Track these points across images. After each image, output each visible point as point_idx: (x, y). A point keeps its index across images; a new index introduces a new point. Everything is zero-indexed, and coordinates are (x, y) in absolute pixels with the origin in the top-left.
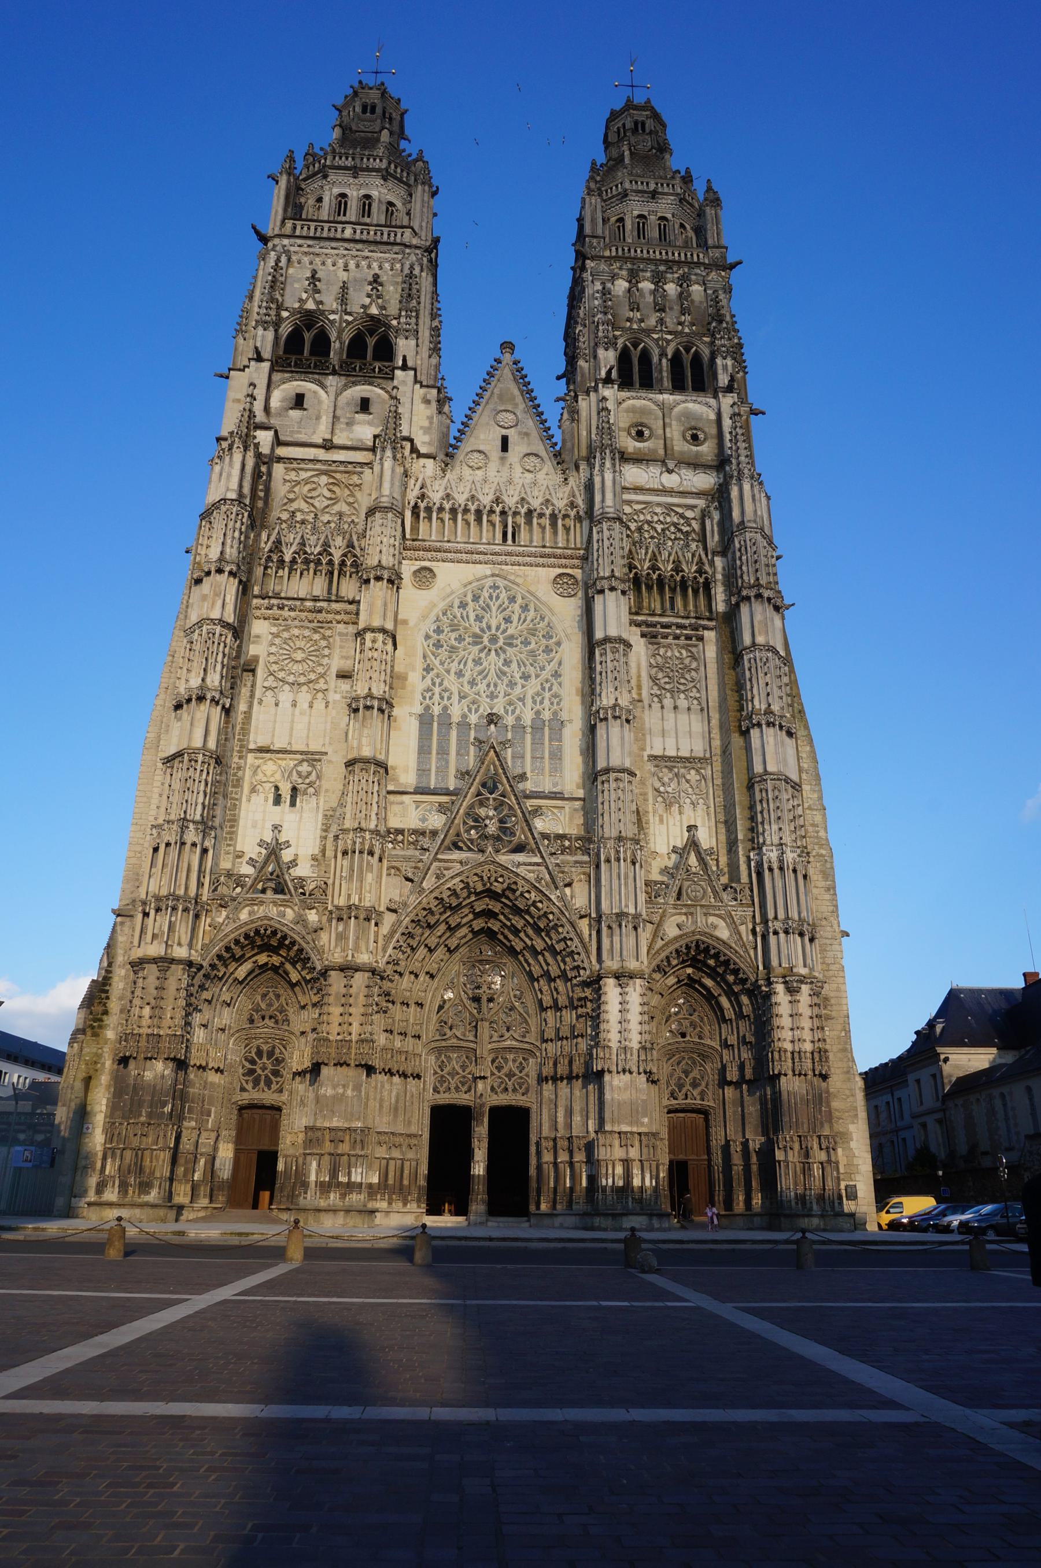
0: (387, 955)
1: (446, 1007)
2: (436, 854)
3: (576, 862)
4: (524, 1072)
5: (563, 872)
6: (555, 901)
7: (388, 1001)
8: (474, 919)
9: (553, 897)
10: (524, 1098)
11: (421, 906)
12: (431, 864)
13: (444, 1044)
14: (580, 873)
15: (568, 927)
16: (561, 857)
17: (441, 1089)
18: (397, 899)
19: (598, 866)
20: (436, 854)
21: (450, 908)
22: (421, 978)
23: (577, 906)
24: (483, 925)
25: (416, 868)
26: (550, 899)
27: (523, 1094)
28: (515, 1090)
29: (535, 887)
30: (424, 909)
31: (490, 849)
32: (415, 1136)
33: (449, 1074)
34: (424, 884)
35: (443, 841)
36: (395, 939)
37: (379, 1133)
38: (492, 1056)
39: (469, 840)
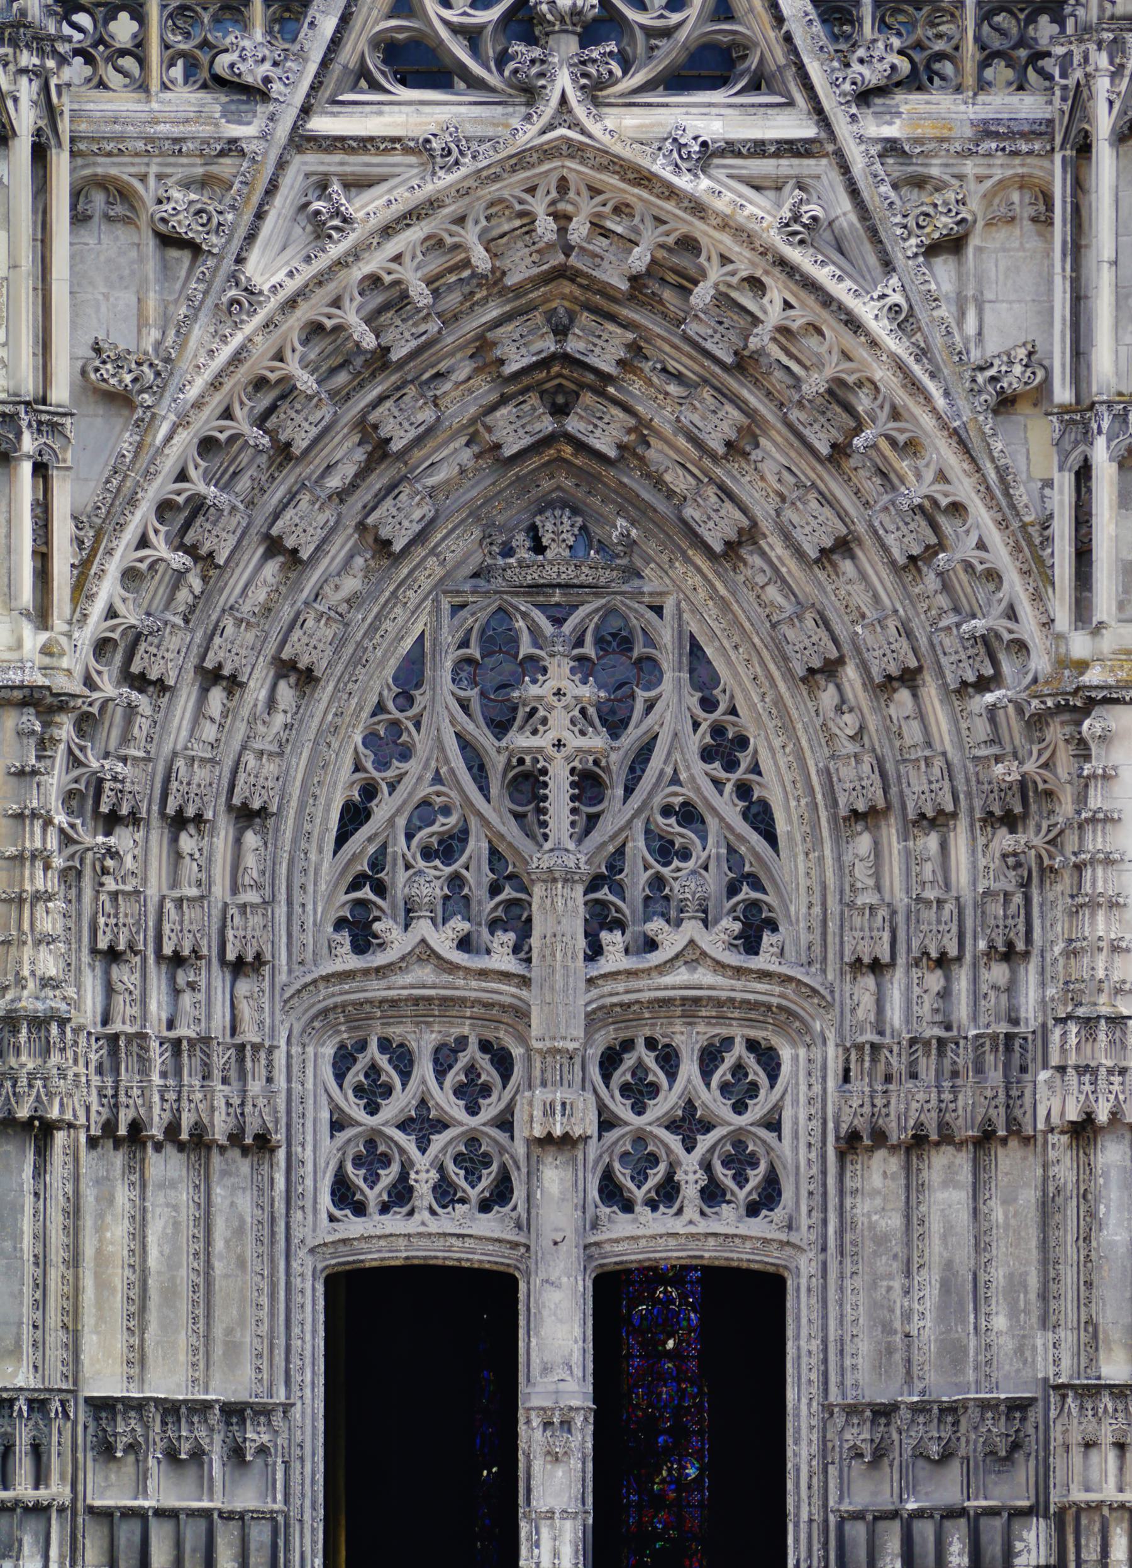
0: (97, 609)
1: (383, 809)
2: (306, 111)
3: (986, 131)
4: (757, 1109)
5: (919, 182)
6: (880, 328)
7: (111, 821)
8: (503, 400)
9: (866, 311)
10: (756, 1227)
11: (243, 374)
12: (282, 165)
13: (376, 989)
14: (1002, 185)
15: (944, 452)
16: (909, 102)
17: (373, 1196)
18: (123, 339)
19: (1084, 148)
20: (306, 111)
21: (380, 359)
22: (257, 690)
23: (993, 345)
24: (547, 424)
25: (204, 183)
26: (853, 324)
27: (753, 1210)
28: (712, 1194)
29: (782, 263)
30: (260, 383)
31: (564, 81)
32: (264, 1412)
33: (403, 1126)
34: (254, 258)
35: (335, 43)
36: (130, 535)
37: (102, 1407)
38: (605, 1038)
39: (456, 30)
